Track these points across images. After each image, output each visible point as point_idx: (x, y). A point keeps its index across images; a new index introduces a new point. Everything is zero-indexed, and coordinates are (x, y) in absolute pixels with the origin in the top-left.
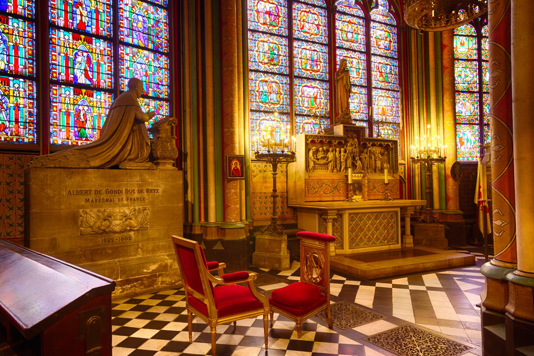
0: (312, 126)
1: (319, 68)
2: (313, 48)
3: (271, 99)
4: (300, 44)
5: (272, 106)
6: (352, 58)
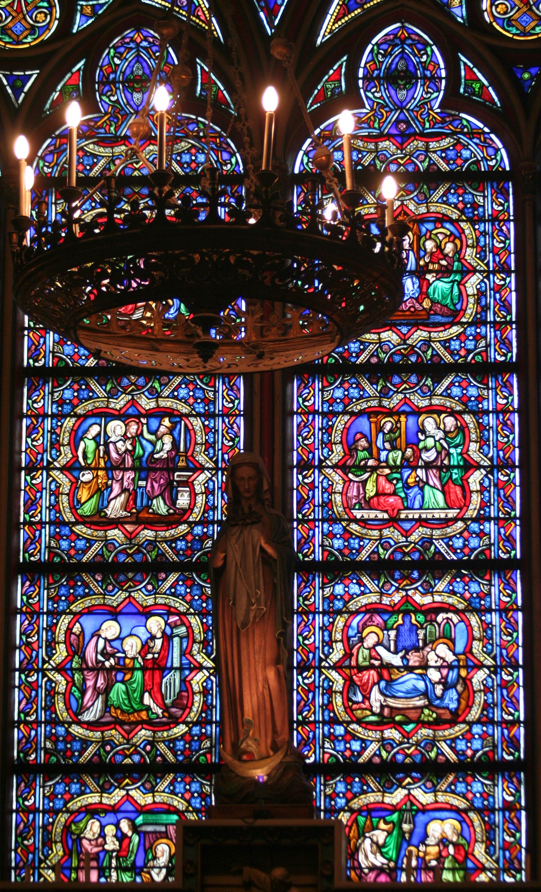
0: (125, 826)
2: (147, 403)
4: (68, 394)
6: (417, 412)
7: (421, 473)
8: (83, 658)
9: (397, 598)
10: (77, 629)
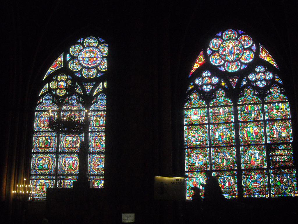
0: (70, 181)
1: (77, 146)
3: (44, 168)
5: (45, 171)
7: (103, 143)
8: (66, 163)
9: (100, 156)
10: (65, 160)
